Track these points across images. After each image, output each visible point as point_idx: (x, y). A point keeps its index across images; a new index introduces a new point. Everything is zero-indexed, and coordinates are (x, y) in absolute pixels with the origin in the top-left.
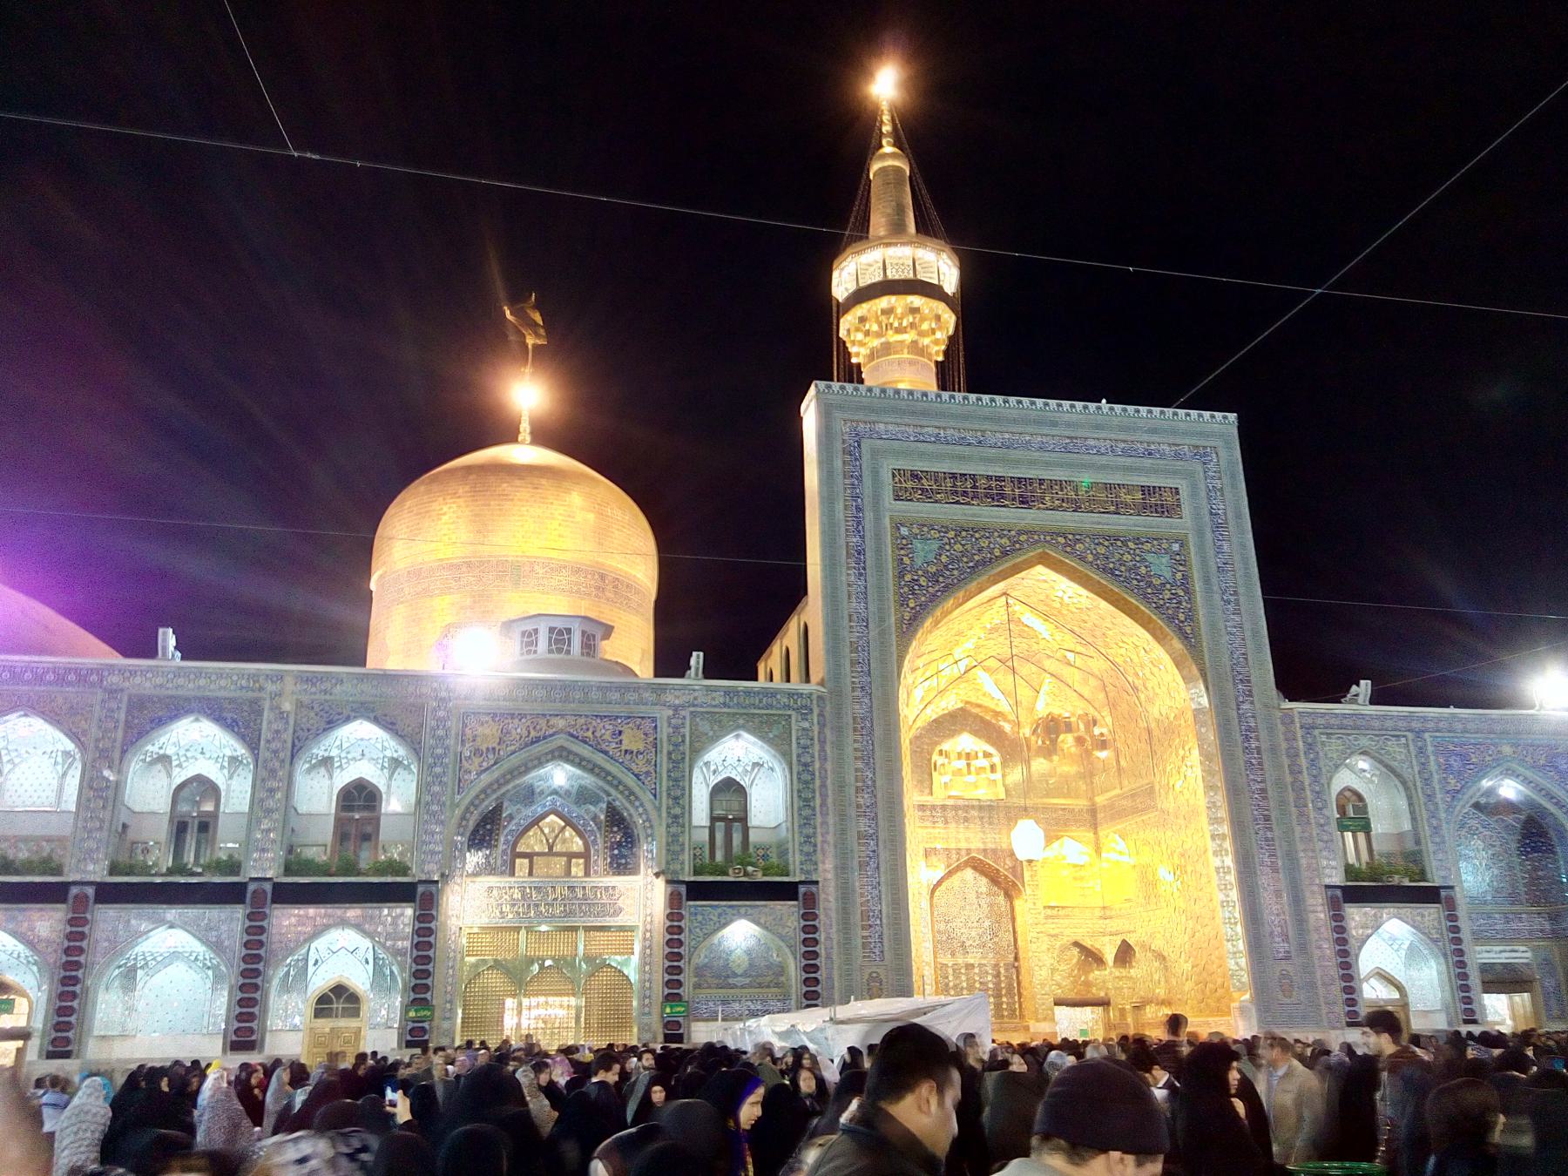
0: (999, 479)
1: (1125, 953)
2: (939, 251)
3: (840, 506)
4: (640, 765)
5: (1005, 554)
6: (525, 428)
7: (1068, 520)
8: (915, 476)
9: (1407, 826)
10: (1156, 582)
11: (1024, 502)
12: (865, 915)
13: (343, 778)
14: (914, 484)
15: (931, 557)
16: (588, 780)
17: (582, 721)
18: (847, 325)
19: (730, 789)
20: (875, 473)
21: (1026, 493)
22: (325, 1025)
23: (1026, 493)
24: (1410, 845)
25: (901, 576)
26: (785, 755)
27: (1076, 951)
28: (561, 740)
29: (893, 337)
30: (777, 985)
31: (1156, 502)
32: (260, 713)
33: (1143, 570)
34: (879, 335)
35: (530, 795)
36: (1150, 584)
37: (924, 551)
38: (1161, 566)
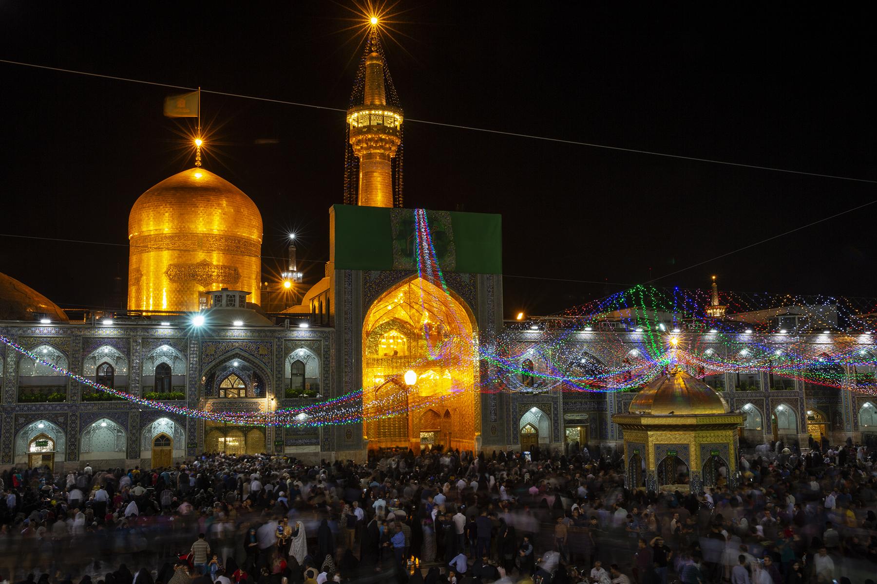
2: (394, 112)
4: (265, 360)
6: (198, 158)
10: (463, 284)
13: (158, 362)
15: (377, 276)
16: (246, 364)
18: (353, 141)
19: (299, 365)
22: (159, 448)
26: (319, 354)
27: (430, 413)
28: (237, 351)
29: (373, 151)
30: (315, 434)
34: (366, 149)
35: (225, 369)
36: (461, 285)
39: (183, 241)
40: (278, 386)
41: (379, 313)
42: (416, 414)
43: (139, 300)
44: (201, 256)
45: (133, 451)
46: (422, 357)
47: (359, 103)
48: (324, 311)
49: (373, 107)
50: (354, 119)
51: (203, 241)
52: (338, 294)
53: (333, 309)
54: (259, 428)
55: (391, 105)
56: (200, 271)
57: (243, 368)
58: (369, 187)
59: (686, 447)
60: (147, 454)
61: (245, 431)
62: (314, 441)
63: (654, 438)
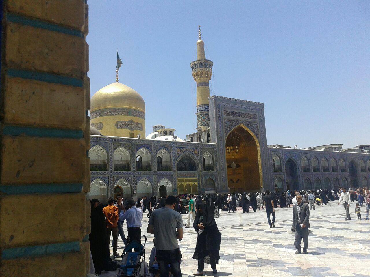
0: (237, 112)
1: (237, 181)
3: (217, 116)
5: (237, 124)
7: (244, 119)
8: (226, 111)
9: (279, 164)
11: (239, 116)
12: (222, 177)
17: (190, 149)
20: (222, 111)
24: (280, 167)
25: (225, 128)
31: (255, 117)
32: (152, 147)
33: (253, 127)
37: (228, 123)
38: (255, 126)
62: (212, 189)
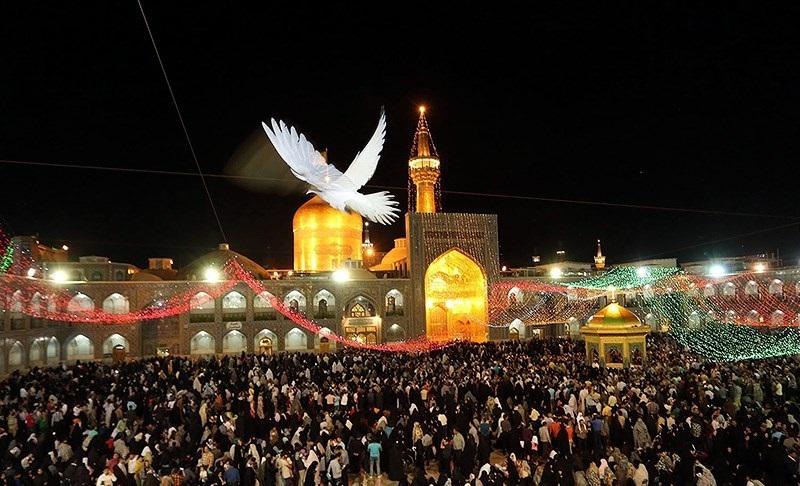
13: (320, 299)
14: (430, 234)
21: (454, 235)
23: (454, 235)
39: (322, 232)
40: (383, 311)
41: (433, 268)
42: (451, 325)
43: (299, 264)
44: (332, 240)
45: (310, 345)
46: (458, 293)
47: (416, 155)
48: (403, 268)
49: (423, 157)
50: (413, 164)
51: (332, 233)
52: (412, 260)
53: (409, 268)
54: (373, 333)
55: (432, 155)
56: (332, 248)
57: (363, 301)
58: (422, 202)
59: (621, 345)
60: (317, 347)
61: (366, 334)
63: (604, 340)
